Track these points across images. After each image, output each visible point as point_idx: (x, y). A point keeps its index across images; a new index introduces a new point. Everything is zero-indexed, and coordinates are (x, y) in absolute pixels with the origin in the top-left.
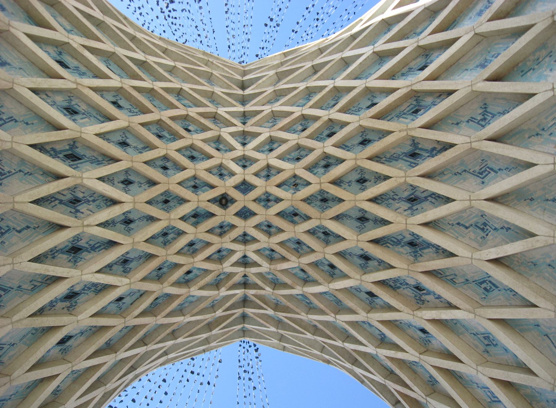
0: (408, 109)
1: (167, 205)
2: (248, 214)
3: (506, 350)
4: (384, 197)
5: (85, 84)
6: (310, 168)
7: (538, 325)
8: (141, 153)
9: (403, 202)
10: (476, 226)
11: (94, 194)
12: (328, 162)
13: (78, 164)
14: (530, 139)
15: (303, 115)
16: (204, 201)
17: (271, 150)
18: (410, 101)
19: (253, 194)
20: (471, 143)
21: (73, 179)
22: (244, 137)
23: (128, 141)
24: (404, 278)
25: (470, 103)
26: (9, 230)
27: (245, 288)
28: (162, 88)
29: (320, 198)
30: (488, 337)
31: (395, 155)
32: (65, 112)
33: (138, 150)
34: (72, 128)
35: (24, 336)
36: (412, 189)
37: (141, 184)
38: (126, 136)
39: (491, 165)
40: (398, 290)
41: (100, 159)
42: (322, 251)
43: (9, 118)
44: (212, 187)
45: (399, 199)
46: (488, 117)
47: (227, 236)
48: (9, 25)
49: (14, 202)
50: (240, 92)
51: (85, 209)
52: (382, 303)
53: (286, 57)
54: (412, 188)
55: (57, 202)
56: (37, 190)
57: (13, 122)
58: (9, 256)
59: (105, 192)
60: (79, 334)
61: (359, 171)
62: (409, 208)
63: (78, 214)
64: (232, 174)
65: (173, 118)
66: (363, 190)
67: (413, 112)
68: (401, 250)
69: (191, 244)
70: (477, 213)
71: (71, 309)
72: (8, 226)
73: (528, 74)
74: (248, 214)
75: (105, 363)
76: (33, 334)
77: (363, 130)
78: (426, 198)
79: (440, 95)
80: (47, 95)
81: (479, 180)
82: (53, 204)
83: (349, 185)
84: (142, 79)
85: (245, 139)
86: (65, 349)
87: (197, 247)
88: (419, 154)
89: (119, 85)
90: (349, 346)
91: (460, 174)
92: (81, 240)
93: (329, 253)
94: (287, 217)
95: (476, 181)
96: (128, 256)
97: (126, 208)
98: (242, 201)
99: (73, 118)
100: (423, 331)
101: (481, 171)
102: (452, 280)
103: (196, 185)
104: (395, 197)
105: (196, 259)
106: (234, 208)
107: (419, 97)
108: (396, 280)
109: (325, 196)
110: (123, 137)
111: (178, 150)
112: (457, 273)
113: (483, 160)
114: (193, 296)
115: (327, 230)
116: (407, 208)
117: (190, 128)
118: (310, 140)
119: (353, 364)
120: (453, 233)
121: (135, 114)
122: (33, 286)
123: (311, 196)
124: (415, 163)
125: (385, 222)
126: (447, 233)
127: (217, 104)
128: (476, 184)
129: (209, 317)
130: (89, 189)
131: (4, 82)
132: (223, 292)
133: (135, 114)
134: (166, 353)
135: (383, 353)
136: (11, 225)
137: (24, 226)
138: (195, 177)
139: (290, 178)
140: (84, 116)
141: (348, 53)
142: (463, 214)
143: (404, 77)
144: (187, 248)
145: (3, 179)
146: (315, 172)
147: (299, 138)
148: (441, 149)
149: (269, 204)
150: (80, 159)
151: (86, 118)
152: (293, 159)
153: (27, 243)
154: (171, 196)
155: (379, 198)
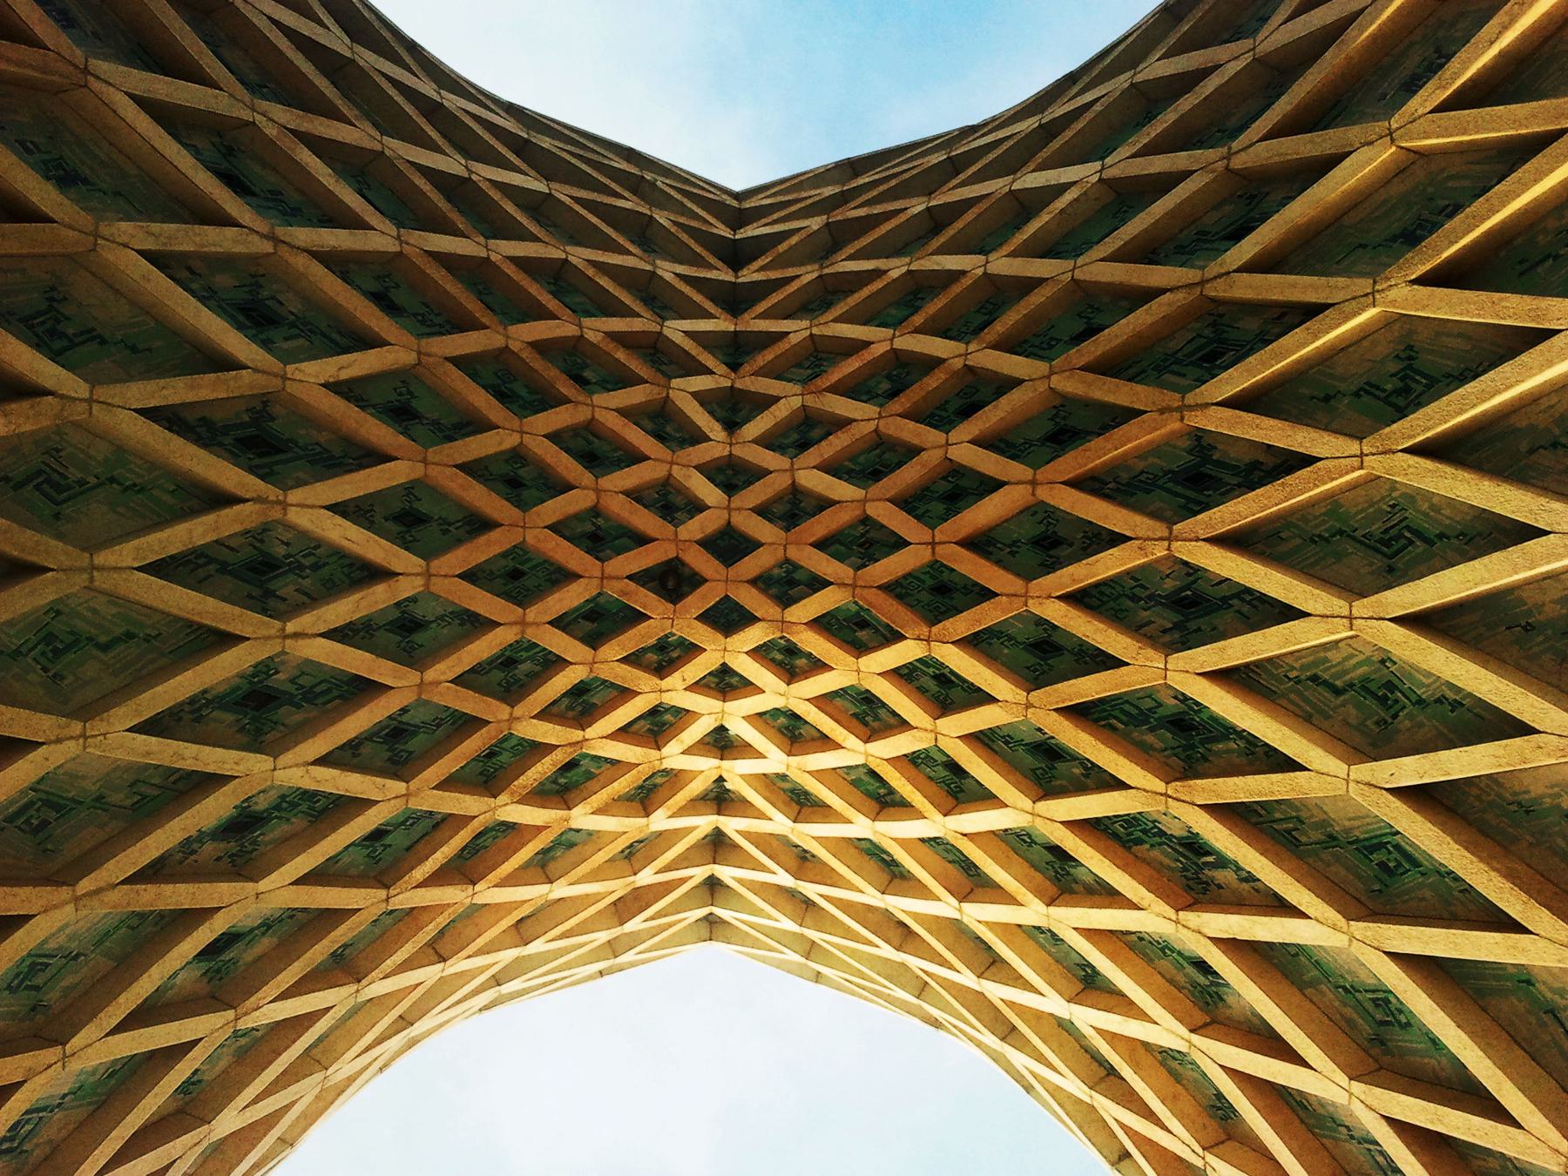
0: (1186, 351)
1: (517, 583)
2: (735, 616)
4: (1108, 591)
5: (298, 243)
6: (908, 503)
7: (1529, 982)
8: (451, 439)
9: (1158, 609)
10: (1364, 688)
11: (316, 548)
12: (959, 488)
13: (277, 463)
14: (1534, 457)
15: (894, 351)
16: (617, 578)
17: (803, 446)
18: (1197, 325)
19: (752, 565)
20: (1362, 455)
21: (257, 506)
22: (733, 409)
23: (414, 403)
24: (1156, 817)
25: (1365, 343)
26: (77, 642)
27: (719, 813)
28: (514, 260)
29: (929, 582)
30: (1387, 1001)
31: (1142, 478)
32: (241, 318)
33: (441, 431)
35: (107, 934)
36: (1188, 574)
37: (450, 524)
38: (409, 392)
40: (1135, 848)
41: (337, 451)
42: (929, 727)
43: (82, 333)
44: (642, 540)
45: (1150, 597)
46: (1413, 385)
47: (677, 675)
48: (86, 71)
49: (94, 568)
50: (726, 275)
51: (291, 588)
52: (1089, 879)
53: (857, 175)
54: (1186, 570)
56: (159, 535)
58: (74, 714)
59: (345, 543)
60: (258, 927)
61: (1040, 516)
62: (1176, 626)
63: (272, 603)
64: (697, 507)
65: (540, 347)
66: (1051, 567)
67: (1205, 359)
68: (1150, 738)
69: (579, 690)
70: (1368, 654)
71: (239, 861)
72: (72, 633)
73: (1539, 270)
74: (735, 616)
75: (328, 1009)
76: (133, 929)
77: (1063, 405)
78: (1225, 599)
79: (1283, 315)
80: (190, 269)
81: (1379, 562)
82: (201, 573)
83: (1013, 553)
84: (456, 232)
85: (734, 409)
86: (218, 971)
87: (594, 700)
88: (1211, 477)
89: (393, 247)
90: (996, 991)
91: (1326, 540)
92: (277, 672)
93: (952, 733)
94: (839, 630)
95: (1371, 564)
96: (405, 718)
97: (406, 588)
99: (263, 336)
100: (1202, 966)
102: (1289, 832)
103: (600, 536)
104: (1137, 591)
105: (591, 732)
106: (699, 601)
107: (1221, 316)
108: (1131, 821)
109: (946, 576)
110: (401, 394)
111: (554, 437)
112: (1304, 815)
113: (1393, 506)
114: (578, 831)
115: (946, 671)
117: (587, 374)
118: (911, 425)
119: (1003, 1039)
120: (1293, 703)
121: (437, 329)
123: (905, 577)
124: (1199, 503)
126: (1284, 702)
127: (665, 307)
128: (1372, 573)
129: (618, 887)
130: (303, 534)
131: (71, 233)
132: (660, 821)
133: (437, 329)
134: (497, 981)
135: (1087, 1018)
136: (80, 625)
137: (118, 631)
138: (595, 511)
139: (852, 526)
140: (295, 331)
141: (1032, 180)
142: (1329, 654)
143: (1184, 258)
144: (566, 701)
145: (64, 501)
146: (919, 512)
147: (880, 417)
148: (1275, 468)
149: (794, 592)
150: (279, 451)
151: (296, 337)
152: (862, 471)
154: (529, 560)
155: (1094, 592)
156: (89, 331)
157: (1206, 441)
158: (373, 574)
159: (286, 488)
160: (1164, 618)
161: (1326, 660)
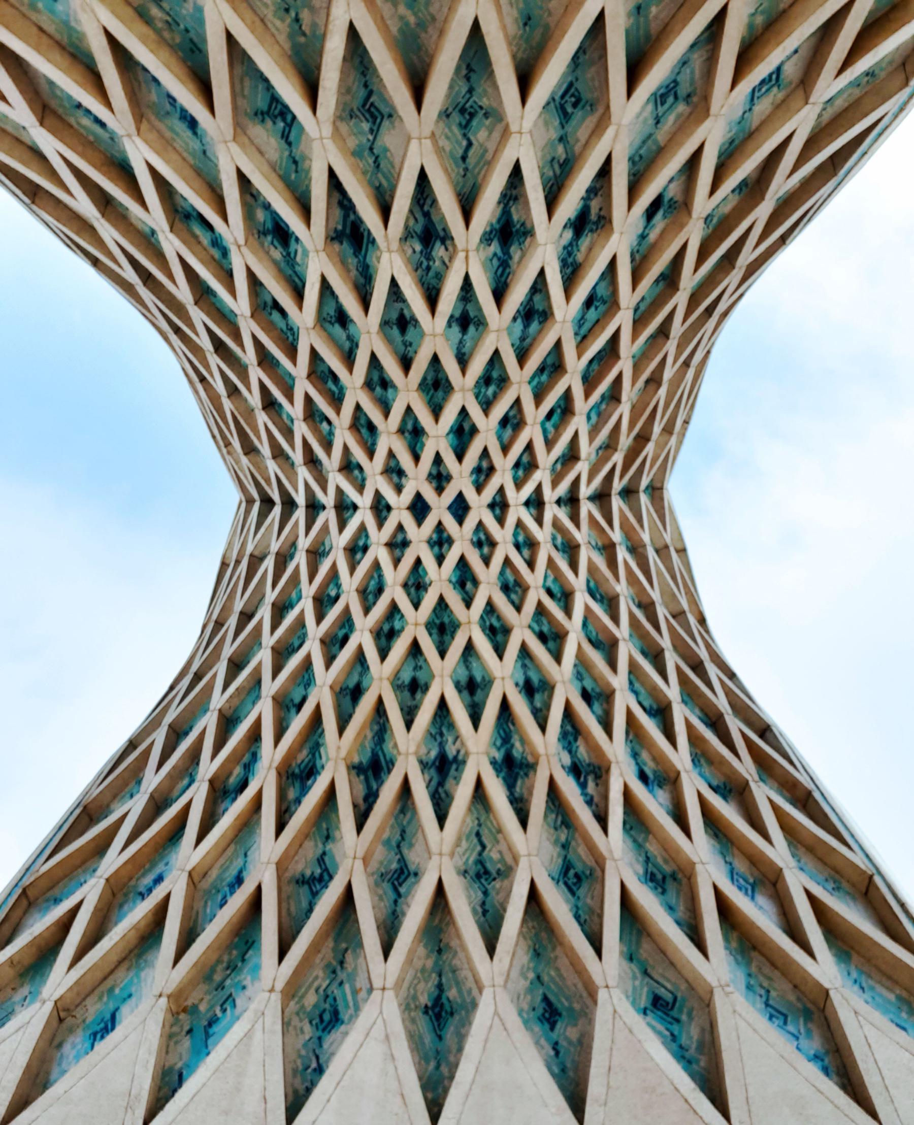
3: (684, 63)
9: (434, 253)
30: (662, 96)
34: (334, 770)
39: (356, 104)
55: (440, 790)
57: (326, 858)
63: (460, 757)
66: (416, 321)
77: (322, 320)
81: (386, 123)
82: (443, 795)
98: (440, 507)
101: (370, 120)
102: (561, 166)
112: (549, 158)
116: (443, 247)
120: (481, 169)
122: (563, 827)
125: (467, 285)
137: (475, 840)
153: (500, 836)
156: (318, 860)
157: (332, 234)
158: (443, 704)
159: (399, 753)
160: (439, 251)
161: (451, 152)
